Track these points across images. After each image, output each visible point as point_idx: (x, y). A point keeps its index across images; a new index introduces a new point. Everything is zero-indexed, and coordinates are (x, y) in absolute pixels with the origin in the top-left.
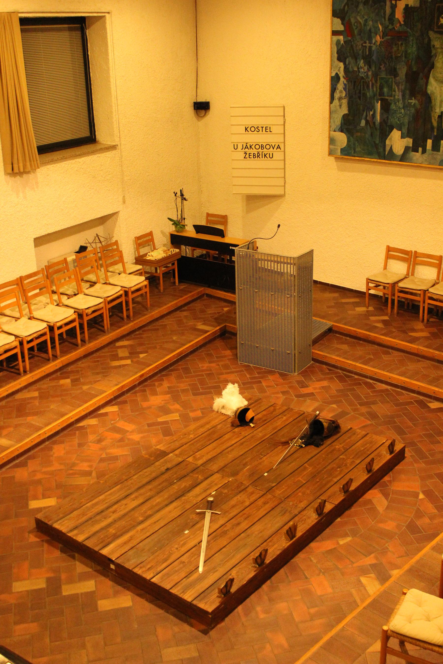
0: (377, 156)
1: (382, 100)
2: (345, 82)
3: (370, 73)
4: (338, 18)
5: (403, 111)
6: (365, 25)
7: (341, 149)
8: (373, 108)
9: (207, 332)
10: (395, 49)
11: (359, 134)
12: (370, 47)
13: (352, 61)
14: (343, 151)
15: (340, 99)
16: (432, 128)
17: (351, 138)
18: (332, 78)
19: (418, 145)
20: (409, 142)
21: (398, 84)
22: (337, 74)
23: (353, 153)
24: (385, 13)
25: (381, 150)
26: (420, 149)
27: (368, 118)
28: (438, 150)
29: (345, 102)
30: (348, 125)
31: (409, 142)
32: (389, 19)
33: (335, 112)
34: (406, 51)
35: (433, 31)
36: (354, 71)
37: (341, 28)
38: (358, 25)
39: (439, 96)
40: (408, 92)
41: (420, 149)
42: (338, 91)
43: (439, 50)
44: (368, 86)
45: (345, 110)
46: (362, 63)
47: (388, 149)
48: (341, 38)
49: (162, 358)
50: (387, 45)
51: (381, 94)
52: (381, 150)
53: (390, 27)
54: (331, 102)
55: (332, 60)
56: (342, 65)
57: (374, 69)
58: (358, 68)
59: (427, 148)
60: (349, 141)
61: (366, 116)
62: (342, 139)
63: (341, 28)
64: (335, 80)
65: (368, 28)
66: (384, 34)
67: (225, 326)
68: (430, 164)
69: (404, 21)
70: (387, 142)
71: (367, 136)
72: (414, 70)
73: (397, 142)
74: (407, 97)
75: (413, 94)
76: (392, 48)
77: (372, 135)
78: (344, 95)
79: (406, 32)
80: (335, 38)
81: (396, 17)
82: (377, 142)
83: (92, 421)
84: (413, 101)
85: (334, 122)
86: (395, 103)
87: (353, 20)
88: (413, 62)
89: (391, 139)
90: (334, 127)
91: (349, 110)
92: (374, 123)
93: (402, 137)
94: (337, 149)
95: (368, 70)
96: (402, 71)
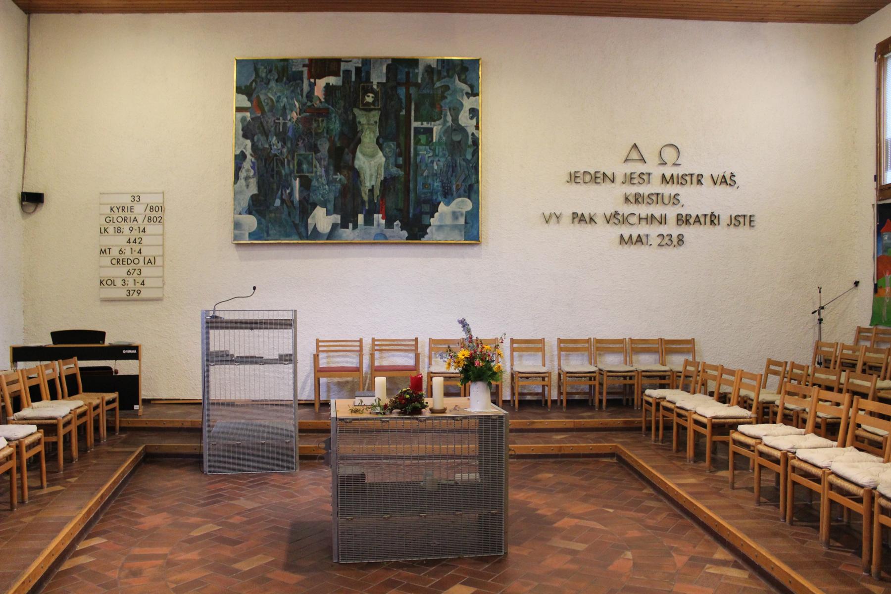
0: (297, 237)
1: (300, 177)
2: (253, 160)
3: (285, 150)
4: (243, 93)
5: (327, 187)
6: (278, 101)
7: (250, 234)
8: (290, 185)
9: (133, 452)
10: (315, 125)
11: (273, 215)
12: (285, 124)
13: (263, 138)
14: (252, 236)
15: (247, 178)
16: (363, 202)
17: (263, 220)
18: (236, 156)
19: (348, 219)
20: (337, 218)
21: (319, 160)
22: (242, 152)
23: (265, 234)
24: (302, 90)
25: (302, 230)
26: (351, 225)
27: (284, 197)
28: (372, 224)
29: (253, 182)
30: (258, 206)
31: (337, 218)
32: (307, 97)
33: (241, 192)
34: (328, 128)
35: (358, 108)
36: (264, 149)
37: (248, 104)
38: (269, 102)
39: (368, 170)
40: (331, 168)
41: (351, 225)
42: (244, 170)
43: (366, 126)
44: (283, 164)
45: (254, 190)
46: (274, 140)
47: (310, 228)
48: (248, 114)
49: (115, 470)
50: (307, 121)
51: (300, 170)
52: (302, 230)
53: (309, 104)
54: (235, 183)
55: (236, 138)
56: (249, 143)
57: (289, 145)
58: (270, 145)
59: (359, 223)
60: (259, 223)
61: (282, 194)
62: (251, 222)
63: (248, 104)
64: (240, 158)
65: (282, 105)
66: (301, 111)
67: (146, 447)
68: (363, 239)
69: (325, 99)
70: (310, 221)
71: (284, 216)
72: (338, 145)
73: (322, 220)
74: (331, 173)
75: (338, 169)
76: (311, 124)
77: (289, 214)
78: (252, 173)
79: (328, 109)
80: (240, 115)
81: (316, 94)
82: (297, 222)
83: (82, 560)
84: (339, 177)
85: (239, 204)
86: (317, 180)
87: (262, 97)
88: (336, 139)
89: (314, 217)
90: (239, 209)
91: (259, 188)
92: (292, 202)
93: (328, 214)
94: (244, 234)
95: (283, 147)
96: (324, 147)
